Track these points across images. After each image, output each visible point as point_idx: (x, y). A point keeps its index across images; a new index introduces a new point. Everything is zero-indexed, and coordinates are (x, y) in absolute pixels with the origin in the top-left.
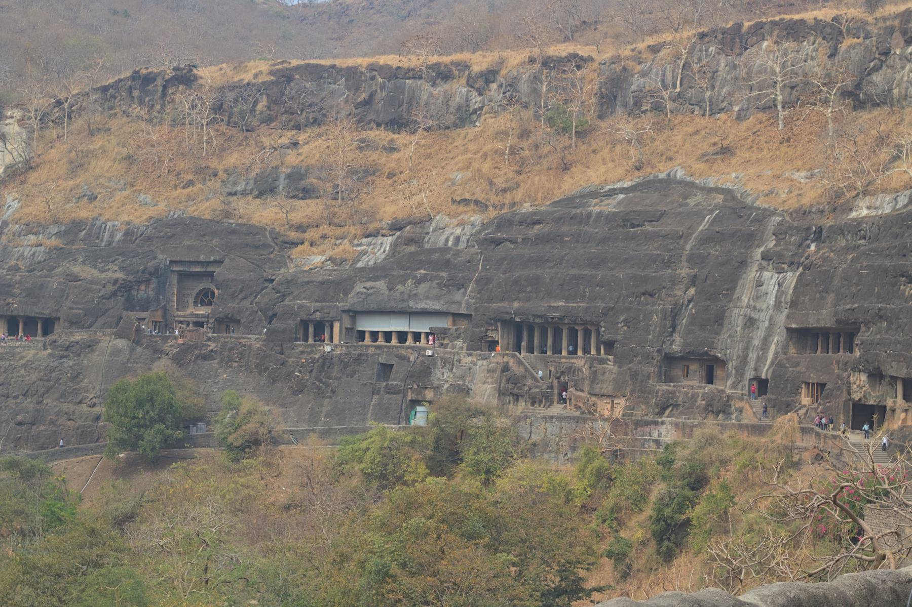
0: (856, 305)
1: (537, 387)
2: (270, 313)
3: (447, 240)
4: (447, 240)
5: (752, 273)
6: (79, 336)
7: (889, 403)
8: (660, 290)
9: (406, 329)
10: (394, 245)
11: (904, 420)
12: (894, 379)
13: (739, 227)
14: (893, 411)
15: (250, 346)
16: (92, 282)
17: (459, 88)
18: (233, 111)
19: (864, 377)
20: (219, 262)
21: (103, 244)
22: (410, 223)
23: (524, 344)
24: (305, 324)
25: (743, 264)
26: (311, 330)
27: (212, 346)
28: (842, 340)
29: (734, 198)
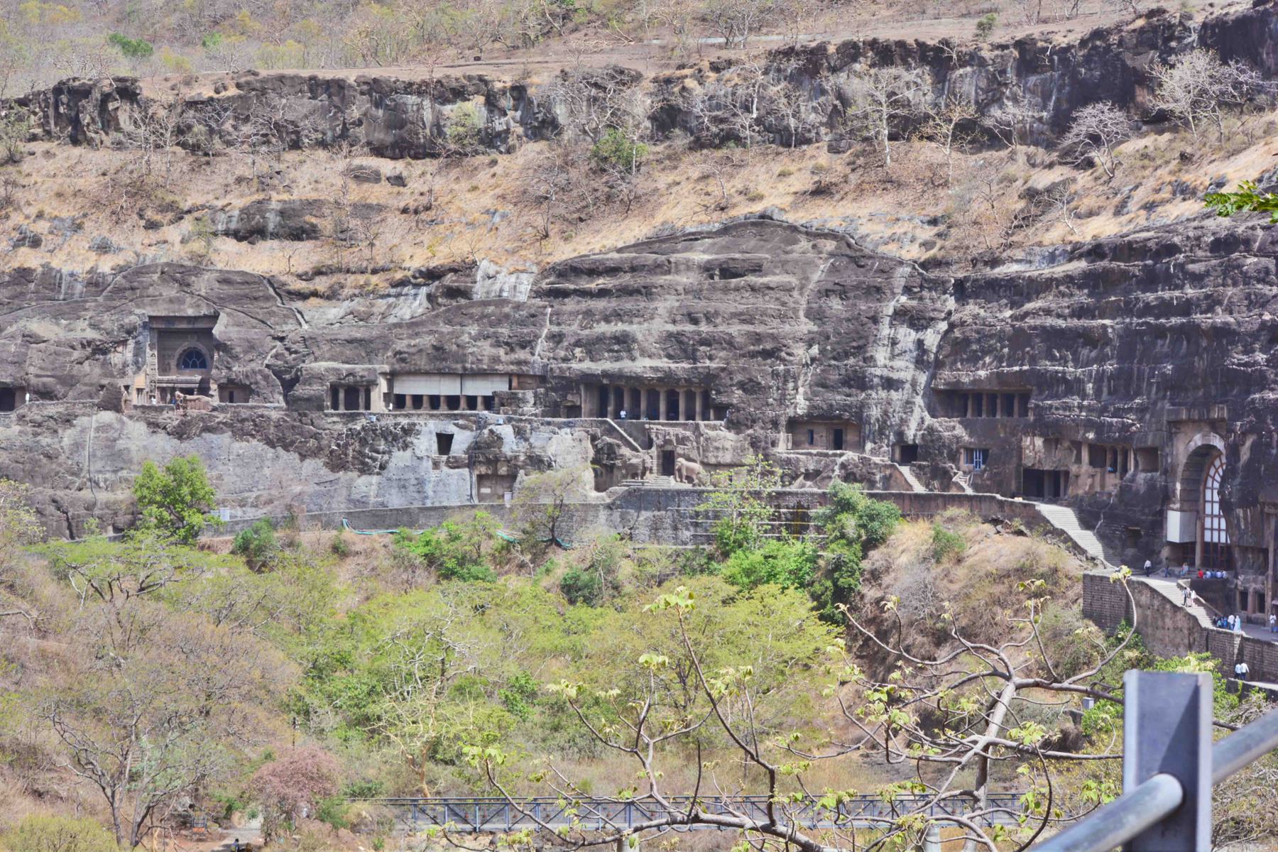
0: (1025, 368)
1: (637, 457)
2: (287, 377)
3: (501, 290)
4: (501, 290)
5: (885, 330)
6: (53, 409)
7: (1074, 469)
8: (780, 350)
9: (457, 393)
10: (430, 297)
11: (1092, 486)
12: (1077, 445)
13: (862, 278)
14: (1077, 476)
15: (269, 418)
16: (58, 344)
17: (474, 108)
18: (197, 130)
19: (1039, 442)
20: (214, 318)
21: (62, 297)
22: (455, 271)
23: (610, 409)
24: (334, 389)
25: (875, 320)
26: (342, 395)
27: (221, 417)
28: (998, 401)
29: (849, 245)
